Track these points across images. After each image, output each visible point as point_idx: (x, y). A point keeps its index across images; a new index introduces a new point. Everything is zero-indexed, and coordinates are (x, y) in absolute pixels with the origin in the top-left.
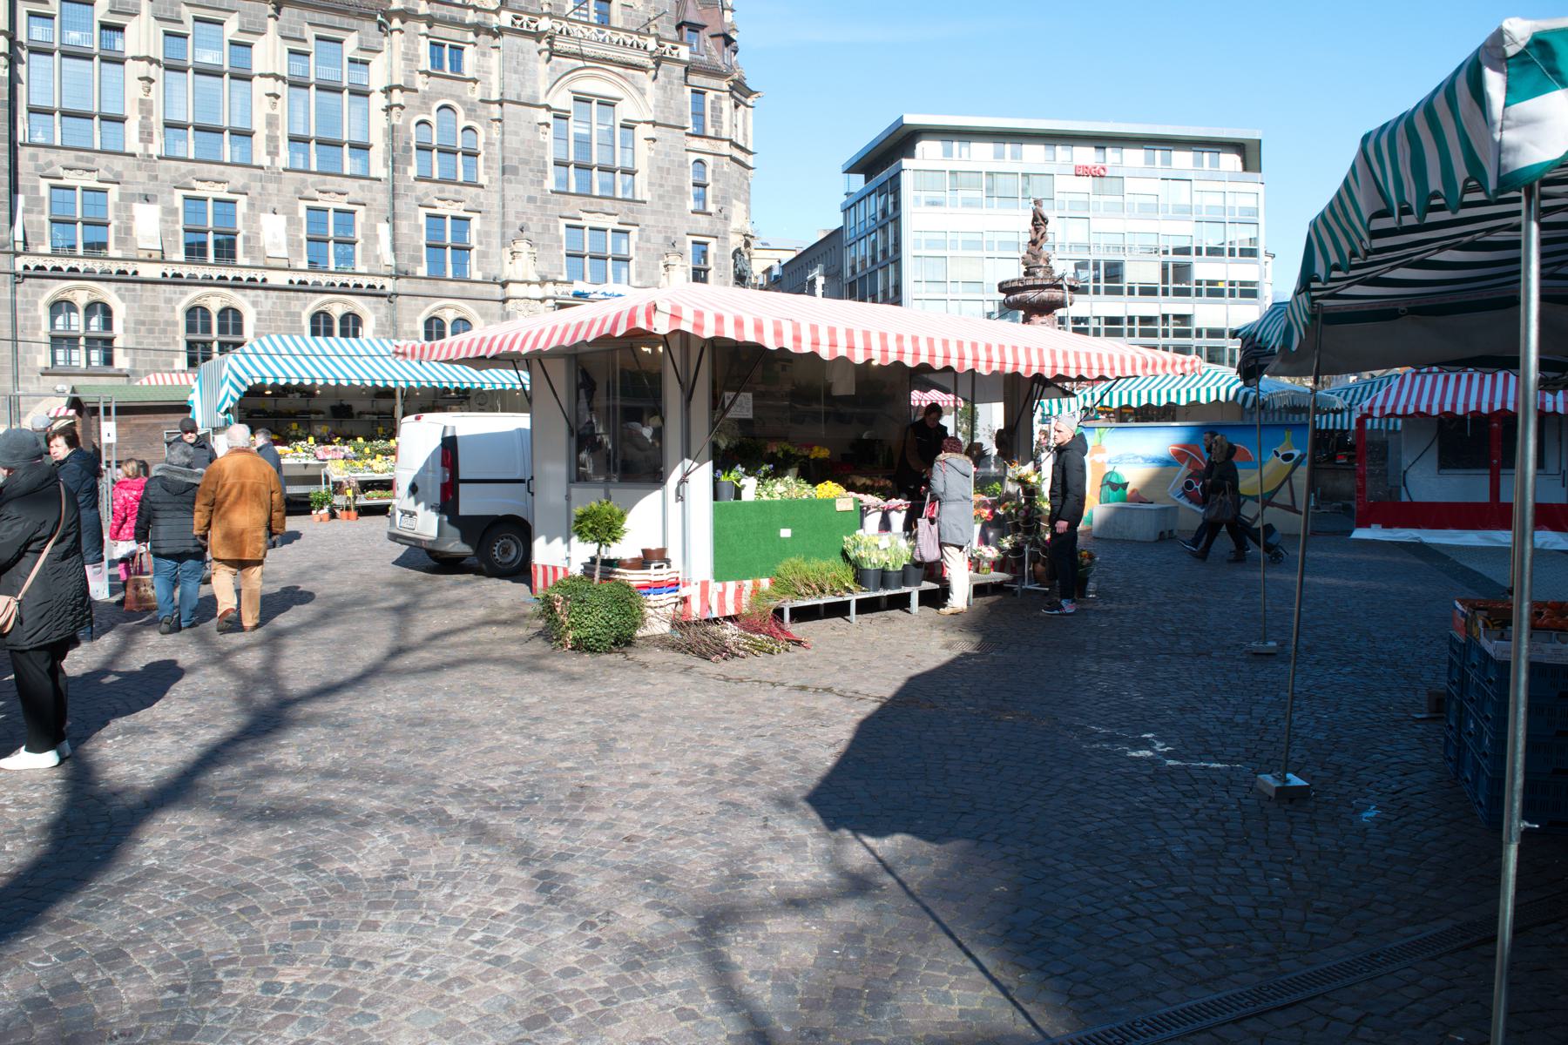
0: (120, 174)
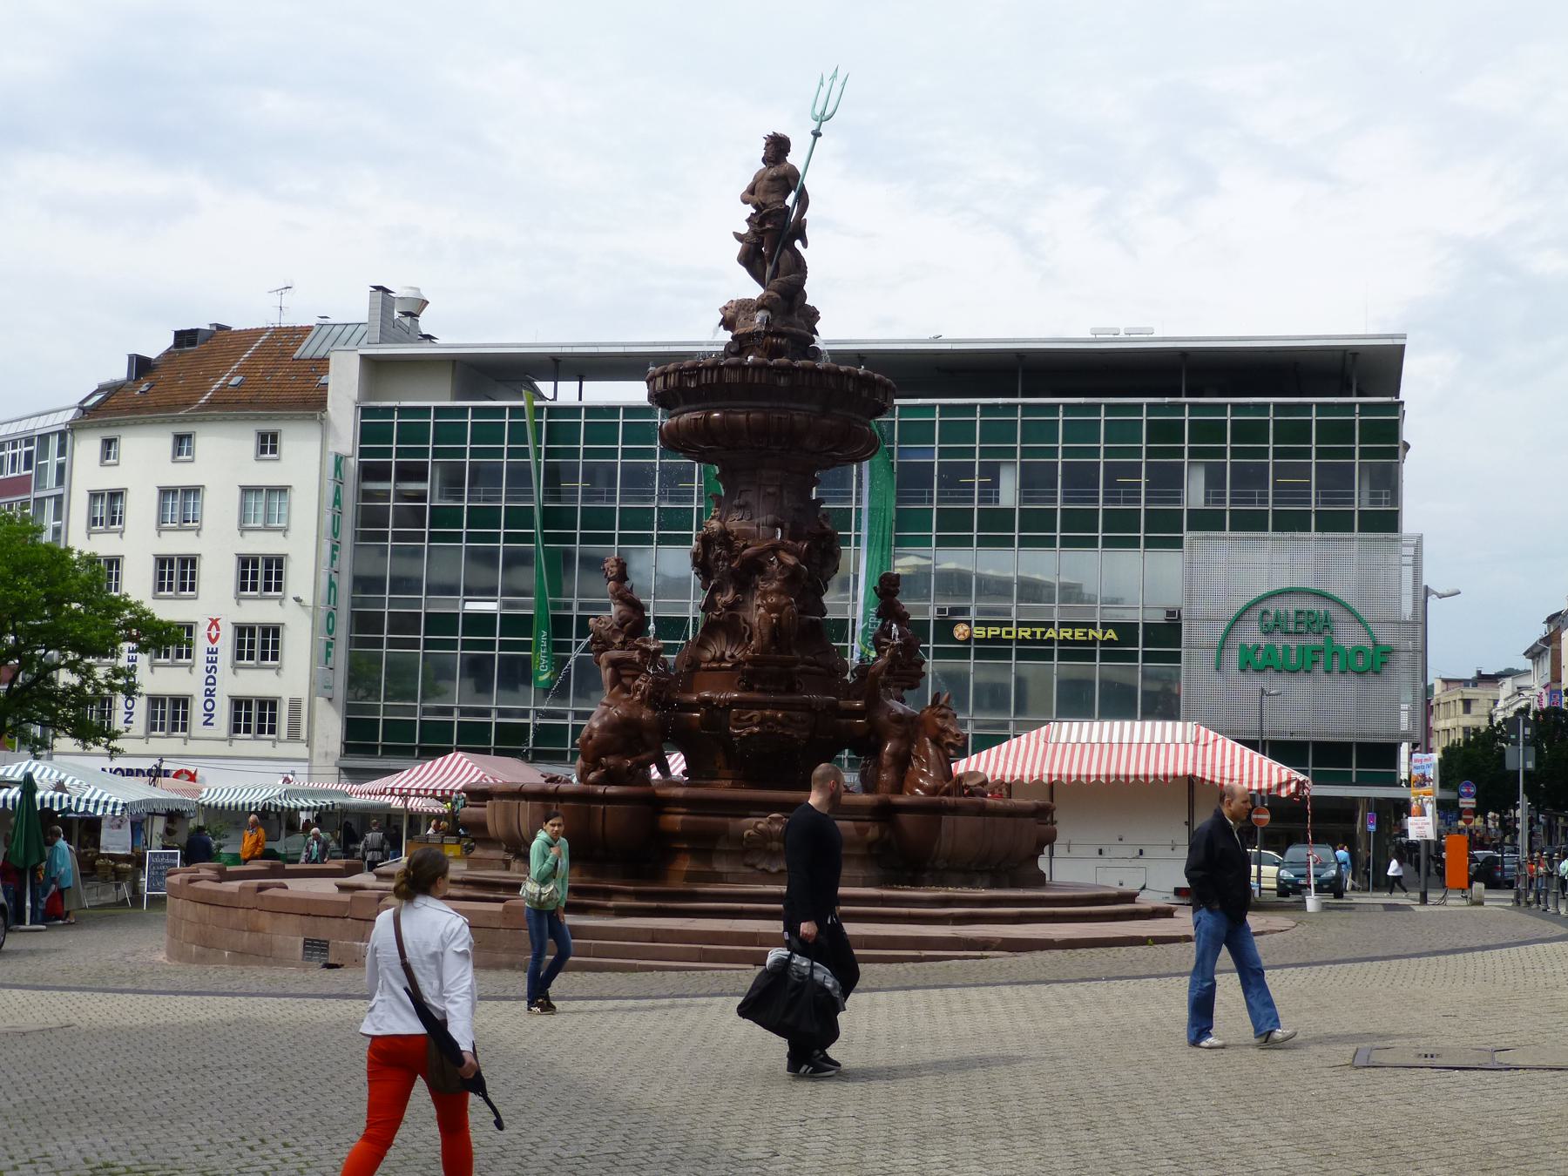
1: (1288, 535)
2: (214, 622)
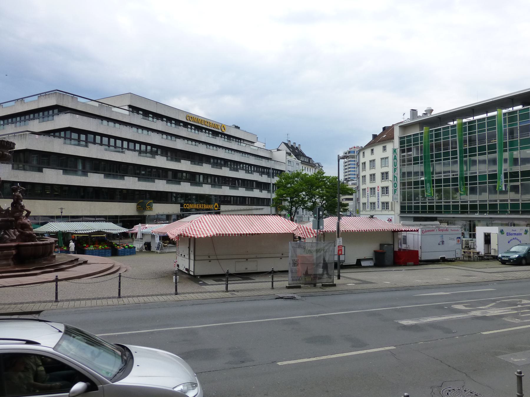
2: (378, 187)
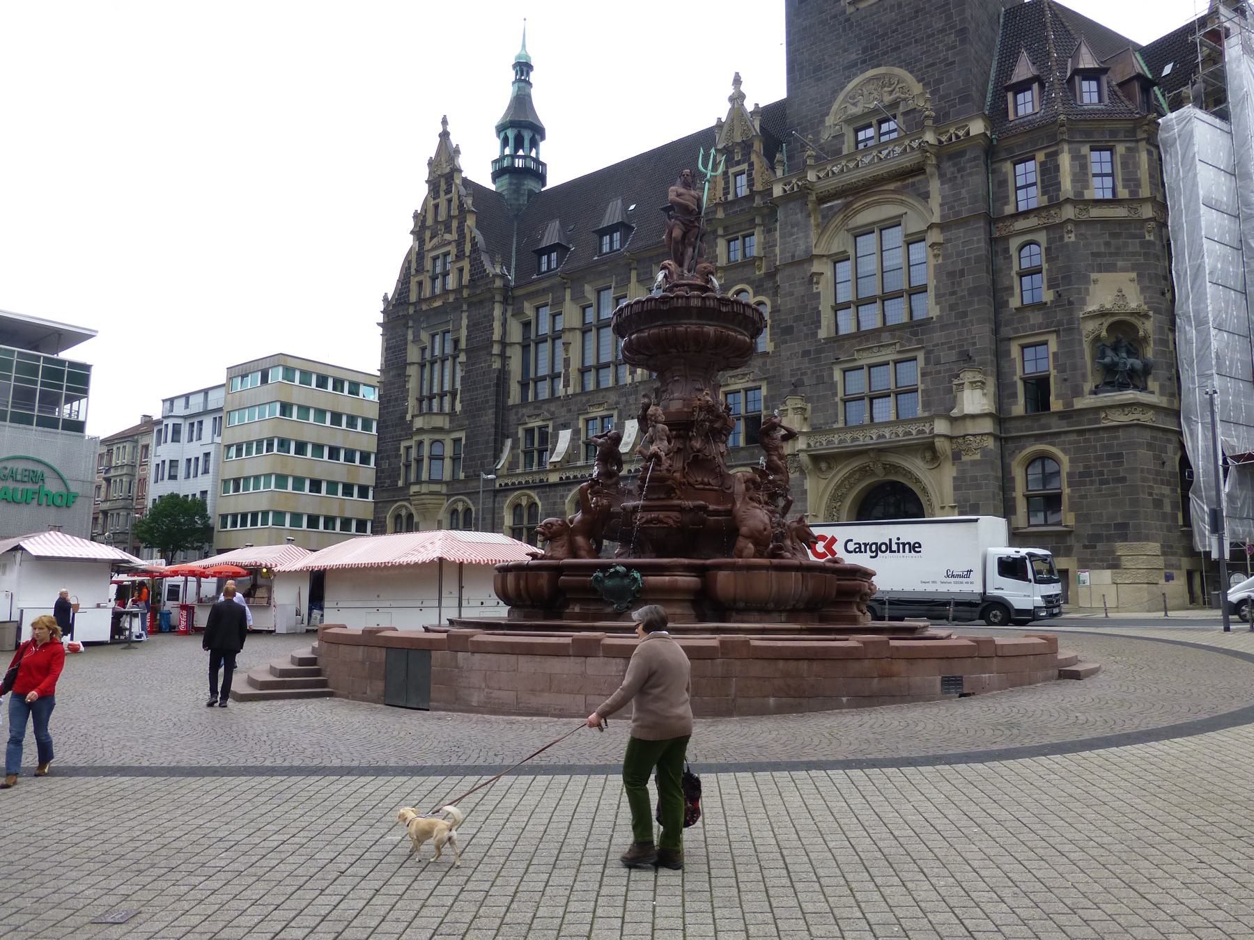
0: (552, 414)
1: (21, 426)
